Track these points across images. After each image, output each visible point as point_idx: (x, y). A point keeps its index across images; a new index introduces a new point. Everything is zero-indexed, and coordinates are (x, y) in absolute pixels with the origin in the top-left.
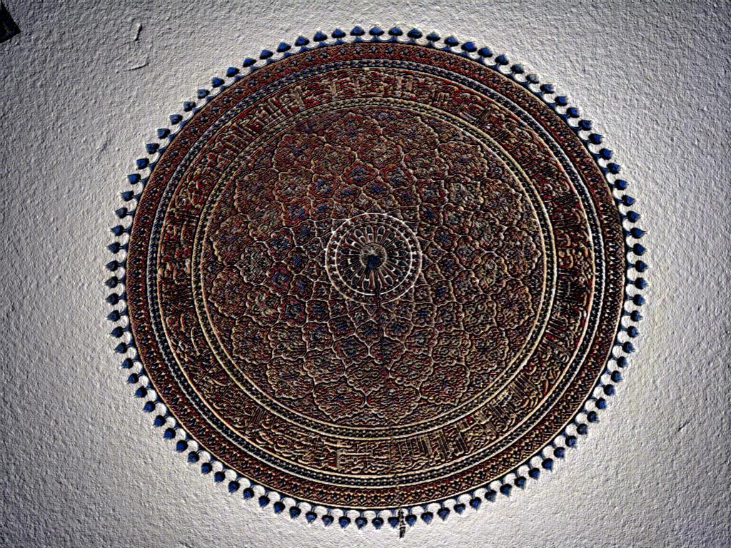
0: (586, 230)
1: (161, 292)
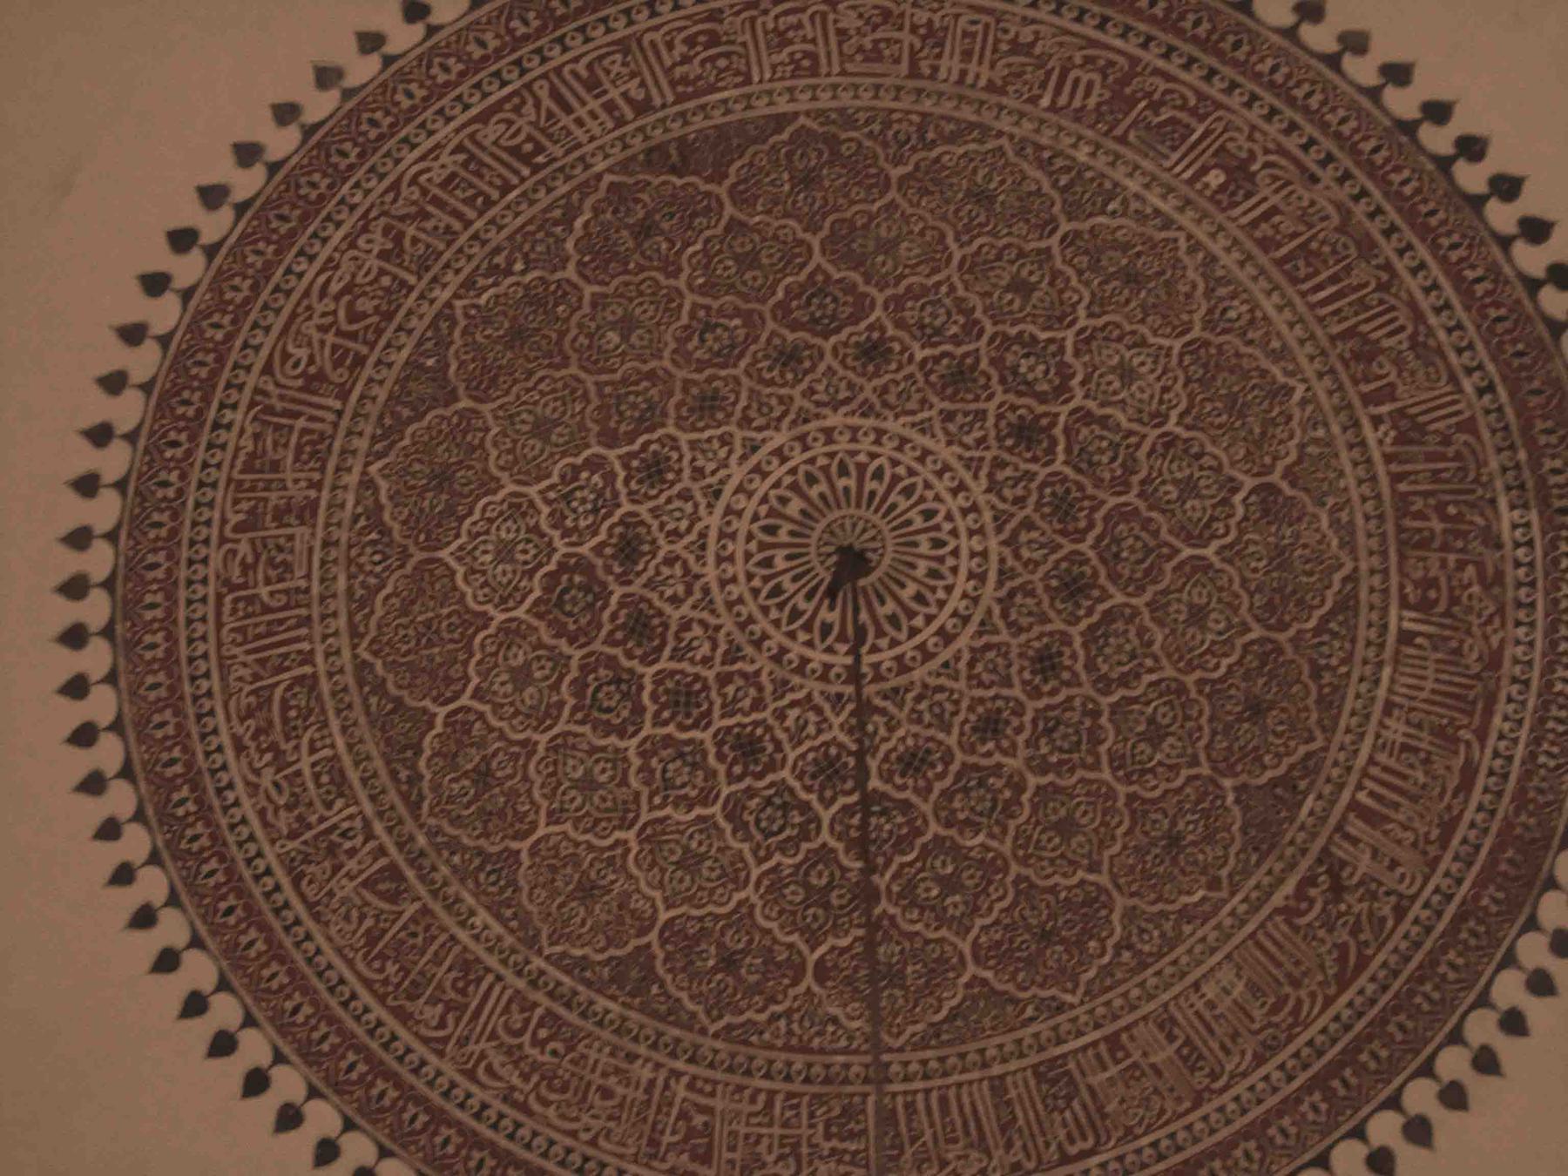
0: (1493, 501)
1: (220, 625)
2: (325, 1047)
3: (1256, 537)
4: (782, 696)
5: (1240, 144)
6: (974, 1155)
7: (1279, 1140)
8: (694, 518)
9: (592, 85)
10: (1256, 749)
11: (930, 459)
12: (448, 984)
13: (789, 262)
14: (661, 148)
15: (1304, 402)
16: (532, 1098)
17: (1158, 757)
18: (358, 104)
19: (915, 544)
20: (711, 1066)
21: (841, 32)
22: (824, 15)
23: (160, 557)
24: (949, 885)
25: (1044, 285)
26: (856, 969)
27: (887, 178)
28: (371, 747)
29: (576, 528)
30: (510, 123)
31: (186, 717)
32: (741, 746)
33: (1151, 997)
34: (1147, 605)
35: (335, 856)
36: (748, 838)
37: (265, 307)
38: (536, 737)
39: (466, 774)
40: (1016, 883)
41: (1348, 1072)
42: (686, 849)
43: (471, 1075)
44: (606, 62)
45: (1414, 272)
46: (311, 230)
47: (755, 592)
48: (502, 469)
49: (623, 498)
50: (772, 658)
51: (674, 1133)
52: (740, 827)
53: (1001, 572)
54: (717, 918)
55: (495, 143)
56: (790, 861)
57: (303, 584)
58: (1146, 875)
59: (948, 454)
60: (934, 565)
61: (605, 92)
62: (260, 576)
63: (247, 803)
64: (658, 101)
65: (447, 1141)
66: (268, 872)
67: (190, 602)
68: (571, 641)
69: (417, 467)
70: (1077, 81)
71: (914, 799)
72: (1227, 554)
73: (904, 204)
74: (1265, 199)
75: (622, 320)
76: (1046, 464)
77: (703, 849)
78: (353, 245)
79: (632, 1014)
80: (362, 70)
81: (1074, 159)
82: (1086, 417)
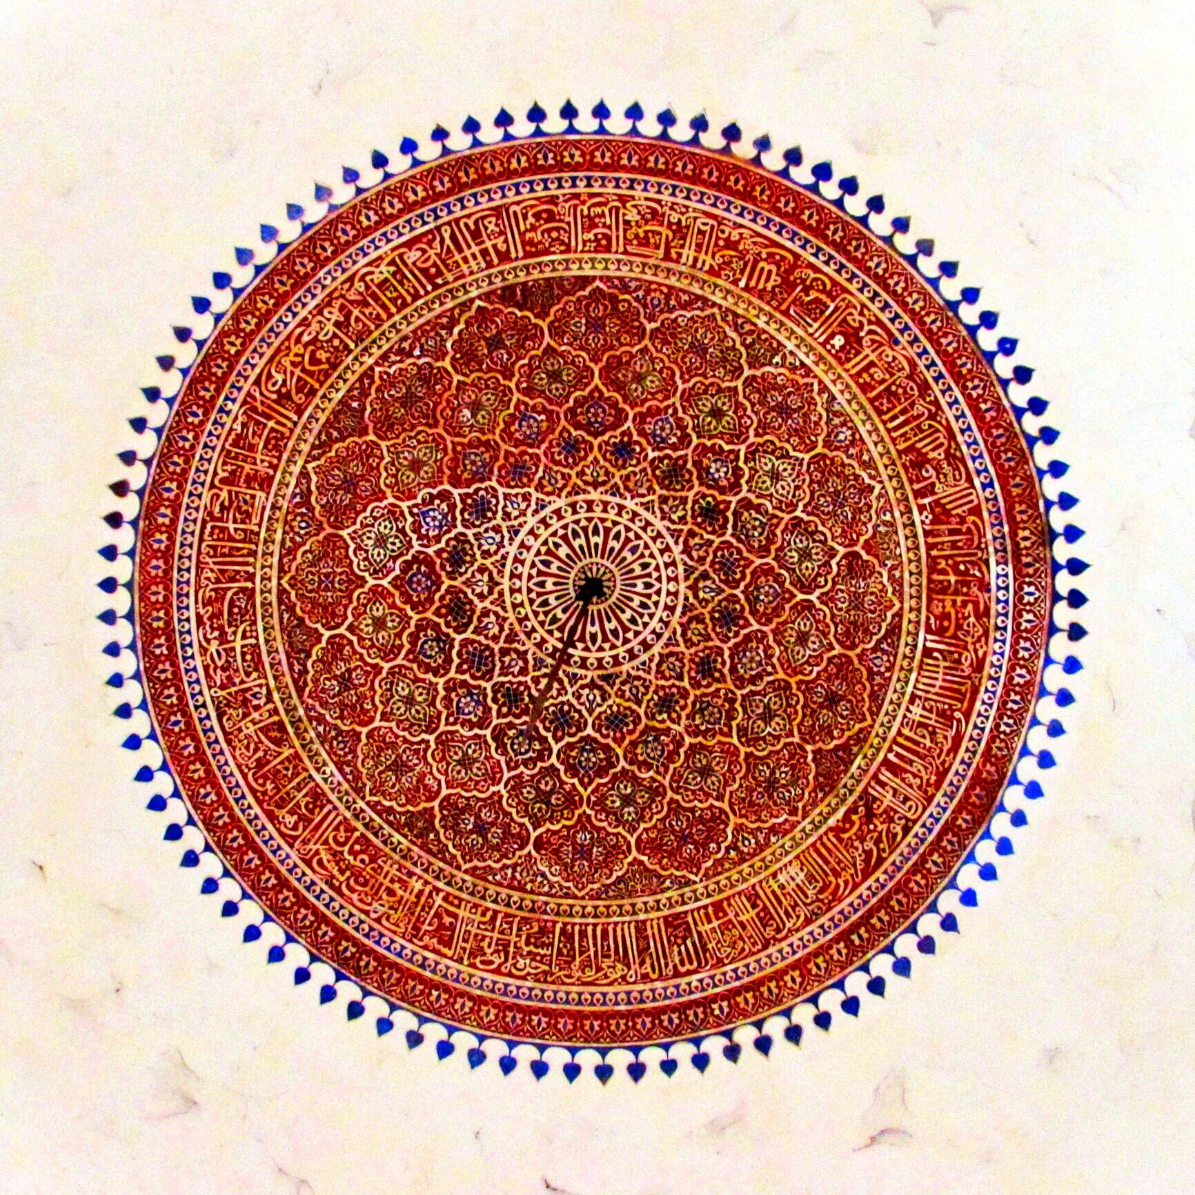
1: (201, 540)
2: (220, 823)
3: (843, 588)
4: (539, 669)
5: (855, 319)
6: (619, 966)
7: (814, 970)
8: (501, 545)
9: (476, 235)
10: (830, 726)
11: (649, 529)
12: (303, 805)
13: (580, 381)
14: (510, 289)
15: (880, 496)
16: (344, 887)
17: (769, 729)
18: (340, 219)
19: (634, 585)
20: (460, 889)
21: (627, 223)
22: (617, 209)
23: (174, 485)
24: (627, 800)
25: (730, 413)
26: (561, 845)
27: (644, 329)
28: (279, 645)
29: (427, 536)
30: (424, 251)
31: (171, 592)
32: (509, 696)
33: (745, 880)
34: (772, 631)
35: (247, 708)
36: (505, 753)
37: (262, 340)
38: (383, 664)
39: (335, 677)
40: (669, 804)
41: (862, 931)
42: (465, 754)
43: (308, 863)
44: (486, 222)
45: (950, 405)
46: (296, 296)
47: (532, 602)
48: (386, 485)
49: (459, 523)
50: (535, 644)
51: (430, 924)
52: (501, 746)
53: (685, 606)
54: (478, 799)
55: (414, 263)
56: (529, 772)
57: (256, 529)
58: (751, 804)
59: (660, 525)
60: (645, 600)
61: (483, 242)
62: (231, 516)
63: (197, 656)
64: (513, 255)
65: (286, 899)
66: (204, 705)
67: (186, 520)
68: (412, 609)
69: (337, 472)
70: (762, 269)
71: (613, 745)
72: (825, 598)
73: (653, 350)
74: (867, 356)
75: (474, 403)
76: (719, 536)
77: (476, 755)
78: (320, 313)
79: (415, 848)
80: (344, 194)
81: (755, 325)
82: (746, 504)
